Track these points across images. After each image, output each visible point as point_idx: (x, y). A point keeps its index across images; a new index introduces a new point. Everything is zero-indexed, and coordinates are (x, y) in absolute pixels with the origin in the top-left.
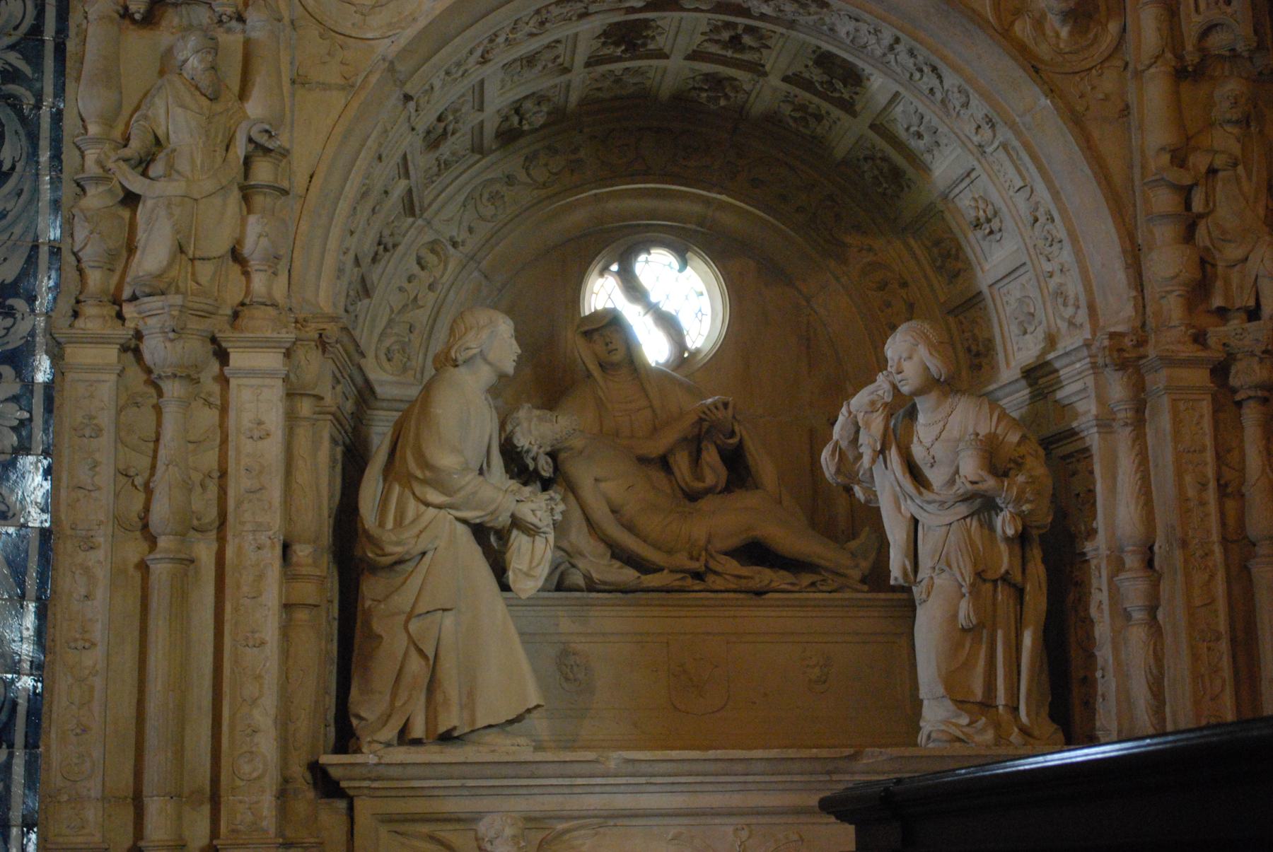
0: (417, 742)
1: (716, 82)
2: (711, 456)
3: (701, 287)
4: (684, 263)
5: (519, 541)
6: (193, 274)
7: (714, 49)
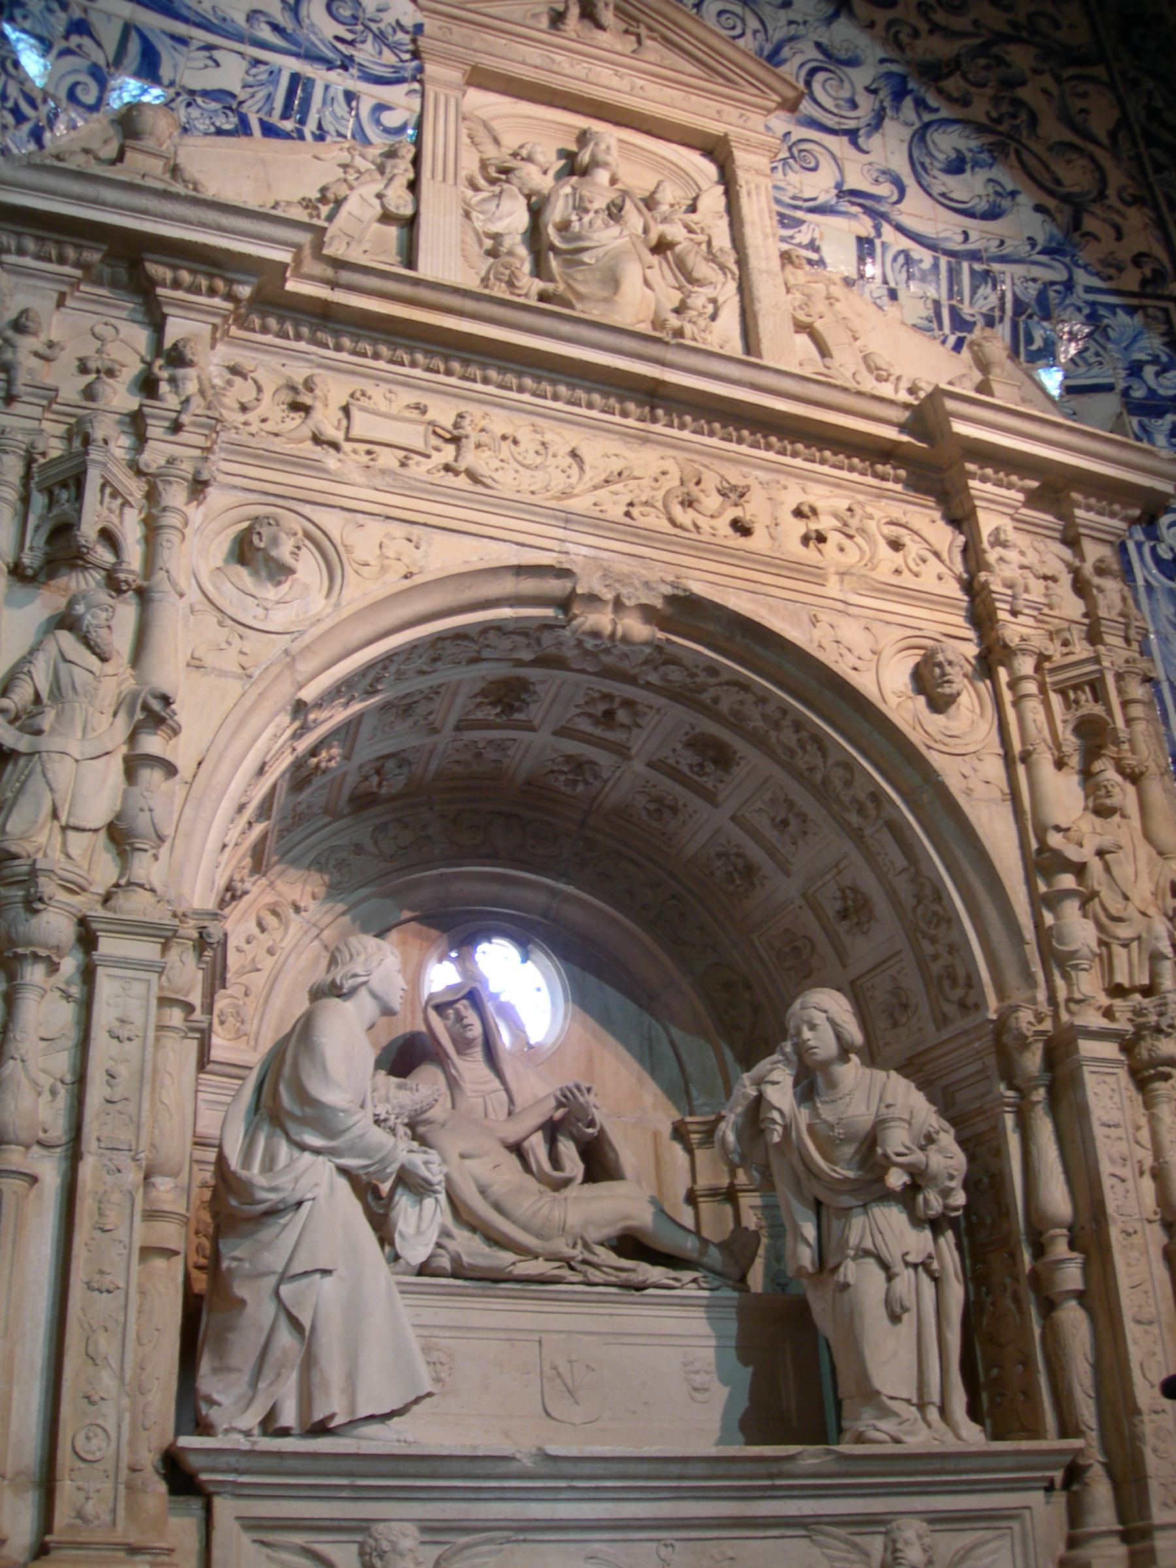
0: (285, 1432)
1: (578, 765)
2: (568, 1149)
3: (541, 982)
4: (525, 958)
5: (404, 1202)
6: (64, 844)
7: (585, 725)
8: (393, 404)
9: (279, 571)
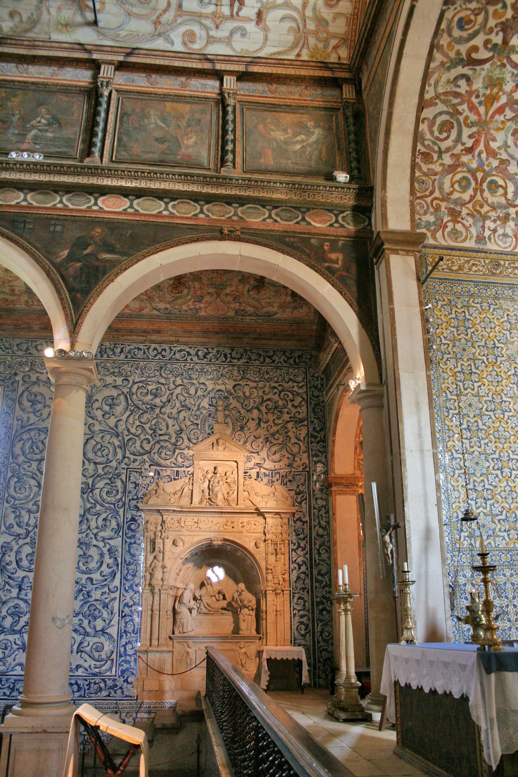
8: (189, 520)
9: (176, 546)
